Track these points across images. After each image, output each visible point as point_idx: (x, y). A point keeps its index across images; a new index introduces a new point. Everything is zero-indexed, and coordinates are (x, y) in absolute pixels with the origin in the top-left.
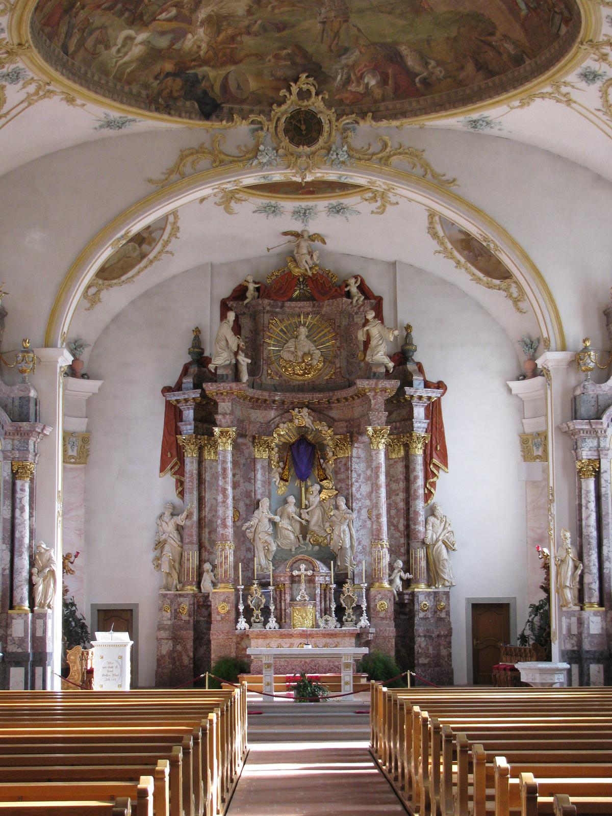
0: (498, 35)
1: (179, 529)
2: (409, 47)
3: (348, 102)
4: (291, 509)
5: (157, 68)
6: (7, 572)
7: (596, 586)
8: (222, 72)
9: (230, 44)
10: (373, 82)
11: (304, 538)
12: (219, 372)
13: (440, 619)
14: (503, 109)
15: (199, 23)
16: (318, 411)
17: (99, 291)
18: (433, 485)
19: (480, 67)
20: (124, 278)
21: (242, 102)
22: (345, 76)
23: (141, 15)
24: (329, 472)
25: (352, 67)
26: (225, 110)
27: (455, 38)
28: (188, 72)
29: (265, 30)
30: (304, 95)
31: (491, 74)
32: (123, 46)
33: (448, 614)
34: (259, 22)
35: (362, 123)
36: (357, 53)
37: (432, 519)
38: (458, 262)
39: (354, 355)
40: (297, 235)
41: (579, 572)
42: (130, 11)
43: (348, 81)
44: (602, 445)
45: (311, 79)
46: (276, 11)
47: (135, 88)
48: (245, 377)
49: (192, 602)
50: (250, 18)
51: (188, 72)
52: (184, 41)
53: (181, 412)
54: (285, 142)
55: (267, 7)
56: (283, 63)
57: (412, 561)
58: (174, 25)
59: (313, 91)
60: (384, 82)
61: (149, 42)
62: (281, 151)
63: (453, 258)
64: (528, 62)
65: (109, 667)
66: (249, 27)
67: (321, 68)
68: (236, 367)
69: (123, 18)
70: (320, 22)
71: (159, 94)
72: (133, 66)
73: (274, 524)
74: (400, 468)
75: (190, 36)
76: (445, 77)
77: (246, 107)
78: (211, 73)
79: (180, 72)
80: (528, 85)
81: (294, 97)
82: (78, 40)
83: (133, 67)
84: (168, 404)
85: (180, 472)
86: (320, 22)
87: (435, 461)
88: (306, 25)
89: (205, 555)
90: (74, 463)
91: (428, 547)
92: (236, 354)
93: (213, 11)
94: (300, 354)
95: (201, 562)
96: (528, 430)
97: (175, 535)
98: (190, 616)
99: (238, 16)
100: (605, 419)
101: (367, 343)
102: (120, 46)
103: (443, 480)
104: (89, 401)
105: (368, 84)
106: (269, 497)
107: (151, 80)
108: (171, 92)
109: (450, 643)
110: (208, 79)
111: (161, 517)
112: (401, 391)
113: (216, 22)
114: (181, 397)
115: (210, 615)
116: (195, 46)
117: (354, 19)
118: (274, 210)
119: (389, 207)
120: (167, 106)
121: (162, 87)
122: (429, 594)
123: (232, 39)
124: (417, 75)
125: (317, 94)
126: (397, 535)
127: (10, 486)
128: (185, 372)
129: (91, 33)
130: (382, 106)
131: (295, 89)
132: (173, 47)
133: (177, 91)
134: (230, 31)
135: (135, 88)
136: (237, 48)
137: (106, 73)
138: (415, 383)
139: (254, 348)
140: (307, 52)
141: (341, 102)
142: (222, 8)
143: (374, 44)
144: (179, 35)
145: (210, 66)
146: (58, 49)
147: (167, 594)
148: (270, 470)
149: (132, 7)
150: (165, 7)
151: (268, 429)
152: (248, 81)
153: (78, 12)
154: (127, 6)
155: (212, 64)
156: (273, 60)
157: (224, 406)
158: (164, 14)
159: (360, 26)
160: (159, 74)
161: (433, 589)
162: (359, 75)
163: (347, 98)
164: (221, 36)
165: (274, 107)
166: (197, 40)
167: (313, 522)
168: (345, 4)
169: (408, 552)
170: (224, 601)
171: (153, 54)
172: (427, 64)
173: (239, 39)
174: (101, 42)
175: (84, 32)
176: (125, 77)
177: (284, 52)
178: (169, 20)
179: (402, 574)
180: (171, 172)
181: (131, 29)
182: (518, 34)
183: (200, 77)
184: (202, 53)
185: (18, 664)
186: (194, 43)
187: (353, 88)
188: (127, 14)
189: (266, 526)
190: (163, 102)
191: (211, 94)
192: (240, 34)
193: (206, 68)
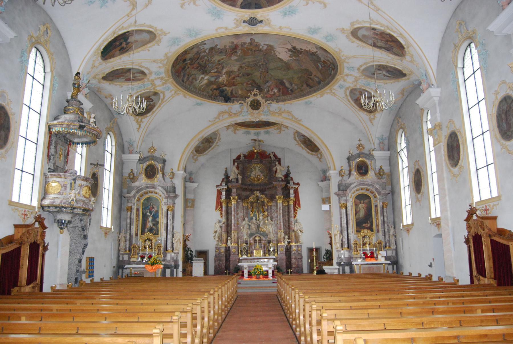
0: (313, 76)
1: (221, 227)
4: (254, 220)
5: (211, 87)
6: (165, 240)
7: (346, 242)
8: (231, 88)
10: (276, 91)
11: (258, 229)
12: (233, 180)
13: (299, 253)
14: (315, 98)
16: (262, 192)
17: (198, 157)
18: (296, 213)
19: (308, 85)
20: (205, 153)
21: (237, 97)
23: (206, 71)
24: (265, 210)
25: (269, 87)
30: (255, 95)
31: (311, 87)
32: (201, 80)
33: (301, 252)
35: (273, 103)
36: (271, 82)
37: (296, 223)
38: (303, 148)
39: (272, 175)
40: (255, 140)
41: (341, 238)
43: (268, 91)
44: (347, 199)
45: (257, 90)
48: (240, 182)
53: (221, 192)
54: (250, 109)
57: (290, 236)
58: (216, 74)
59: (258, 94)
60: (279, 91)
62: (249, 112)
63: (301, 146)
64: (322, 83)
66: (238, 75)
68: (237, 179)
71: (212, 95)
73: (249, 225)
74: (286, 208)
75: (221, 77)
76: (298, 89)
77: (238, 99)
78: (228, 89)
80: (322, 90)
81: (252, 96)
84: (218, 190)
85: (221, 210)
87: (297, 206)
88: (256, 74)
89: (229, 235)
91: (295, 232)
92: (238, 175)
94: (256, 175)
95: (228, 237)
96: (324, 197)
97: (220, 229)
100: (348, 191)
101: (276, 172)
103: (300, 212)
104: (194, 190)
106: (248, 217)
107: (209, 91)
109: (302, 260)
111: (216, 223)
112: (286, 186)
113: (229, 73)
114: (221, 188)
115: (230, 253)
117: (270, 72)
118: (249, 133)
119: (282, 131)
120: (214, 98)
122: (296, 246)
123: (234, 78)
124: (289, 88)
125: (259, 95)
126: (286, 228)
127: (166, 213)
128: (223, 181)
129: (191, 76)
130: (279, 98)
131: (253, 93)
134: (233, 76)
138: (291, 183)
139: (243, 174)
141: (266, 97)
143: (276, 80)
144: (218, 77)
146: (181, 81)
148: (248, 209)
149: (203, 68)
151: (247, 197)
157: (234, 190)
161: (297, 244)
165: (247, 98)
167: (261, 225)
169: (289, 233)
171: (210, 83)
172: (292, 85)
177: (249, 82)
178: (215, 72)
179: (287, 240)
180: (216, 118)
182: (319, 75)
184: (225, 83)
185: (168, 268)
187: (270, 93)
188: (202, 70)
189: (246, 226)
193: (226, 87)
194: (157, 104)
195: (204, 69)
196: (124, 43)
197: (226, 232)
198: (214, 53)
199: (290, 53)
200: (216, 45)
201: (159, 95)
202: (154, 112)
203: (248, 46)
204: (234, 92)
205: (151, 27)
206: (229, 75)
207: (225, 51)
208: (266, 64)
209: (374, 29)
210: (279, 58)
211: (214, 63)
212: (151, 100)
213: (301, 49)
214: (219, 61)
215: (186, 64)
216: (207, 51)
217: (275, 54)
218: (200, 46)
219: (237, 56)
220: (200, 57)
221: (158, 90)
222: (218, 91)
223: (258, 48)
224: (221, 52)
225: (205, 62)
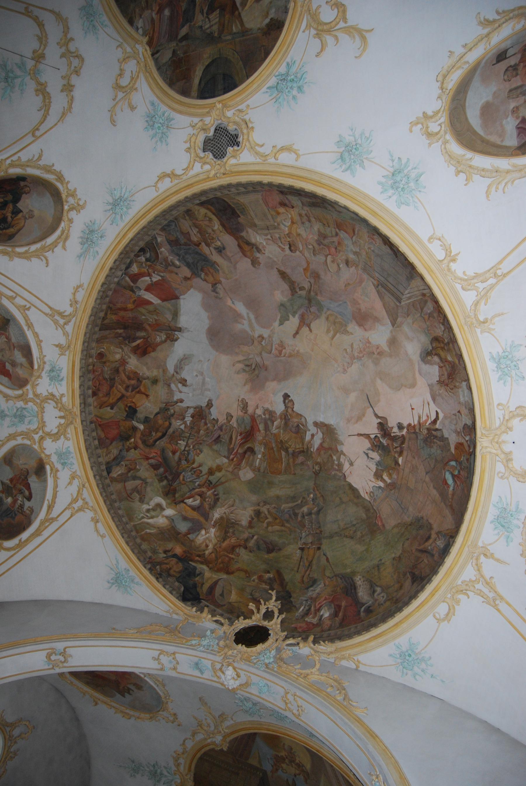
2: (363, 577)
3: (300, 630)
8: (216, 576)
9: (229, 553)
10: (327, 615)
15: (213, 522)
21: (219, 606)
22: (307, 608)
23: (175, 491)
25: (314, 600)
26: (201, 604)
27: (400, 557)
28: (190, 563)
29: (259, 548)
32: (154, 510)
34: (255, 537)
36: (322, 585)
42: (168, 480)
43: (307, 613)
46: (270, 528)
47: (144, 546)
50: (250, 530)
51: (190, 563)
52: (198, 535)
55: (264, 522)
56: (264, 586)
58: (195, 515)
61: (173, 520)
66: (247, 540)
67: (290, 597)
69: (161, 484)
70: (300, 549)
71: (160, 563)
72: (152, 531)
75: (203, 532)
77: (219, 611)
78: (207, 574)
79: (183, 559)
82: (121, 475)
83: (152, 531)
86: (300, 549)
93: (225, 513)
99: (241, 526)
102: (151, 507)
105: (322, 616)
107: (161, 551)
108: (170, 569)
110: (203, 578)
116: (204, 544)
121: (165, 562)
123: (233, 549)
124: (363, 604)
129: (135, 478)
132: (189, 536)
133: (175, 571)
134: (233, 540)
135: (144, 546)
136: (233, 558)
137: (131, 519)
140: (284, 580)
142: (232, 513)
144: (196, 527)
145: (208, 567)
150: (193, 492)
152: (231, 592)
153: (131, 449)
154: (167, 474)
155: (210, 565)
156: (256, 581)
158: (191, 500)
159: (329, 554)
160: (169, 551)
162: (318, 607)
163: (300, 627)
164: (226, 543)
166: (207, 538)
168: (320, 527)
172: (374, 592)
173: (237, 550)
174: (138, 492)
175: (129, 471)
176: (143, 533)
177: (267, 576)
178: (193, 508)
181: (165, 500)
183: (197, 572)
184: (207, 552)
186: (205, 540)
188: (165, 483)
190: (159, 570)
191: (198, 589)
192: (240, 546)
193: (204, 567)
194: (36, 518)
195: (174, 480)
196: (11, 207)
198: (202, 432)
199: (376, 456)
200: (210, 405)
201: (45, 481)
202: (21, 545)
203: (278, 427)
204: (218, 591)
205: (60, 178)
206: (226, 532)
207: (226, 438)
208: (318, 512)
209: (501, 56)
210: (350, 486)
211: (197, 472)
212: (27, 493)
213: (400, 427)
214: (211, 472)
215: (135, 429)
216: (188, 419)
217: (340, 466)
218: (173, 386)
219: (254, 470)
220: (171, 430)
221: (47, 452)
222: (180, 565)
223: (303, 439)
224: (218, 440)
225: (180, 459)
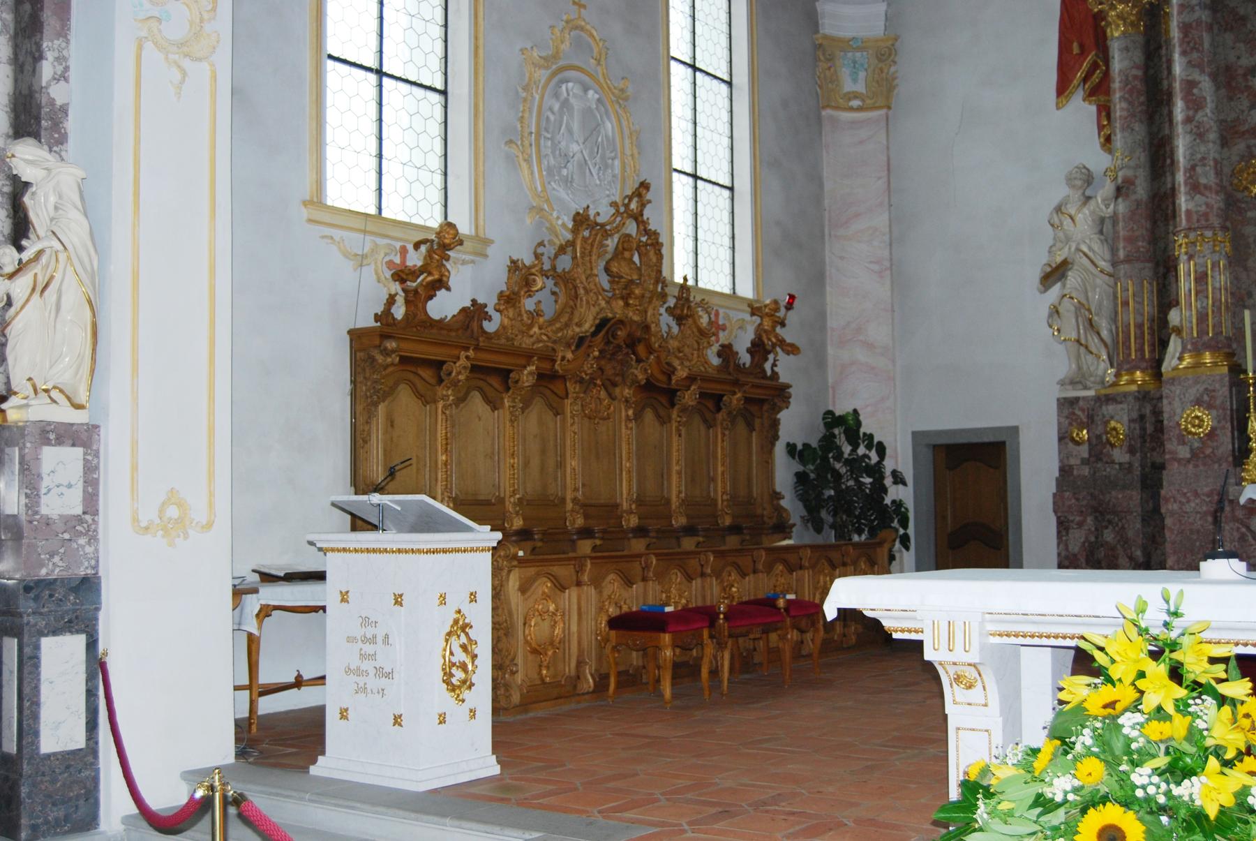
49: (1135, 415)
65: (365, 640)
90: (859, 109)
98: (1131, 450)
147: (1077, 399)
170: (1198, 402)
197: (1147, 270)
